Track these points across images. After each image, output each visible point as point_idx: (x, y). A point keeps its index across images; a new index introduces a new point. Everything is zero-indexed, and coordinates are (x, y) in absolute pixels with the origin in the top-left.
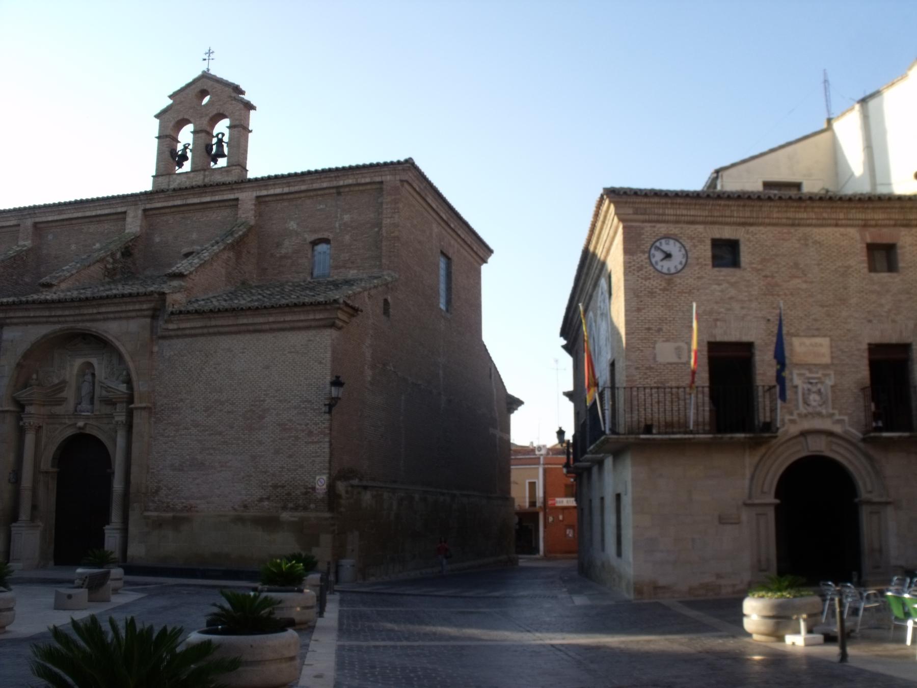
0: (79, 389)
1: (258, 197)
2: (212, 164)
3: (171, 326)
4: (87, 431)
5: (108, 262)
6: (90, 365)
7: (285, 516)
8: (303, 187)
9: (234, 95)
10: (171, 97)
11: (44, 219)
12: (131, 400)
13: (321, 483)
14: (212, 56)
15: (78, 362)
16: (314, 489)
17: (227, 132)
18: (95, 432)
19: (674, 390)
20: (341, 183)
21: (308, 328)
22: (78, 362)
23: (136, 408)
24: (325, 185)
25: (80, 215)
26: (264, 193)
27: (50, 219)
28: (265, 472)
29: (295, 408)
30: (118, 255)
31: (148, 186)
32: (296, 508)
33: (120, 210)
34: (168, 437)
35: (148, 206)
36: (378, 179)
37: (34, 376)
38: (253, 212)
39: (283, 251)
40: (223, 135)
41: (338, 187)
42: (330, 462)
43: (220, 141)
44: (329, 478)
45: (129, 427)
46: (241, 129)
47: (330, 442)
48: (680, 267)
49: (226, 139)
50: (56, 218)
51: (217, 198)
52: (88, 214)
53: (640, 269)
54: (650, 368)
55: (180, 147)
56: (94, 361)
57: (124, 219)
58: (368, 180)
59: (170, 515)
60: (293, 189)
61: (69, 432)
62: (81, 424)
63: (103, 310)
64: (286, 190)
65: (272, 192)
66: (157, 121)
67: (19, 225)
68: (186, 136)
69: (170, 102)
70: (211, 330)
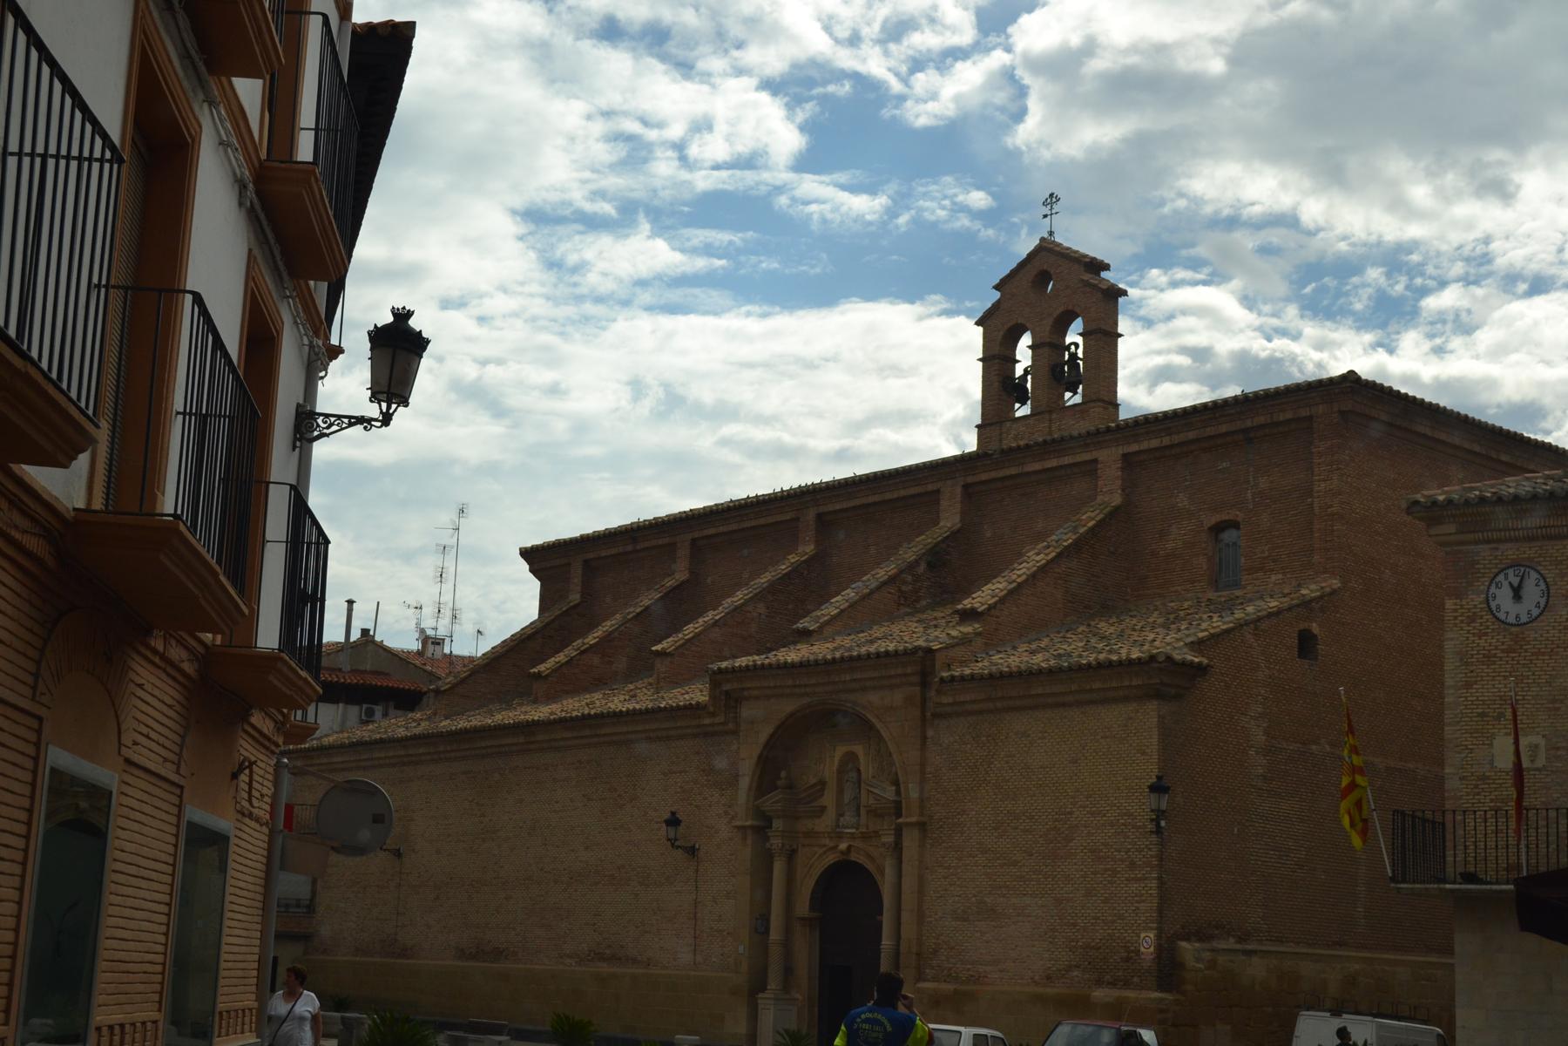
0: (840, 791)
1: (1124, 455)
2: (1068, 395)
3: (945, 700)
4: (853, 857)
5: (905, 582)
6: (851, 757)
7: (1099, 994)
8: (1191, 435)
9: (1087, 277)
10: (997, 287)
11: (830, 508)
12: (898, 810)
13: (1147, 943)
14: (1056, 208)
15: (841, 750)
16: (1138, 952)
17: (1079, 340)
18: (862, 860)
19: (1552, 814)
20: (1249, 423)
21: (1126, 699)
22: (841, 750)
23: (908, 824)
24: (1224, 428)
25: (876, 498)
26: (1135, 447)
27: (838, 507)
28: (1074, 925)
29: (1112, 825)
30: (922, 568)
31: (971, 443)
32: (1112, 984)
33: (930, 487)
34: (949, 868)
35: (970, 479)
36: (1304, 413)
37: (783, 774)
38: (1119, 482)
39: (1170, 545)
40: (1077, 346)
41: (1245, 431)
42: (1160, 911)
43: (1074, 356)
44: (1159, 937)
45: (897, 847)
46: (1104, 338)
47: (1160, 879)
48: (1535, 612)
49: (1080, 355)
50: (845, 505)
51: (1067, 460)
52: (888, 496)
53: (1471, 620)
54: (1484, 778)
55: (1019, 371)
56: (859, 749)
57: (938, 502)
58: (1289, 415)
59: (950, 987)
60: (1176, 439)
61: (831, 859)
62: (843, 846)
63: (858, 676)
64: (1166, 441)
65: (1145, 445)
66: (980, 329)
67: (798, 519)
68: (1024, 354)
69: (997, 295)
70: (999, 705)
